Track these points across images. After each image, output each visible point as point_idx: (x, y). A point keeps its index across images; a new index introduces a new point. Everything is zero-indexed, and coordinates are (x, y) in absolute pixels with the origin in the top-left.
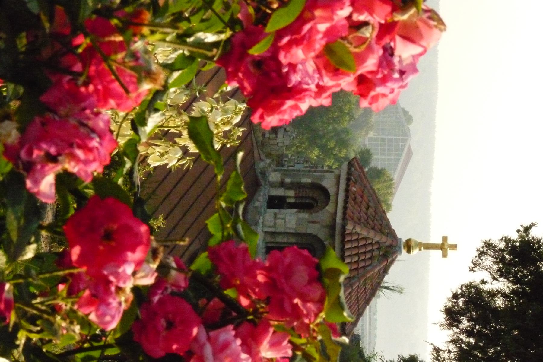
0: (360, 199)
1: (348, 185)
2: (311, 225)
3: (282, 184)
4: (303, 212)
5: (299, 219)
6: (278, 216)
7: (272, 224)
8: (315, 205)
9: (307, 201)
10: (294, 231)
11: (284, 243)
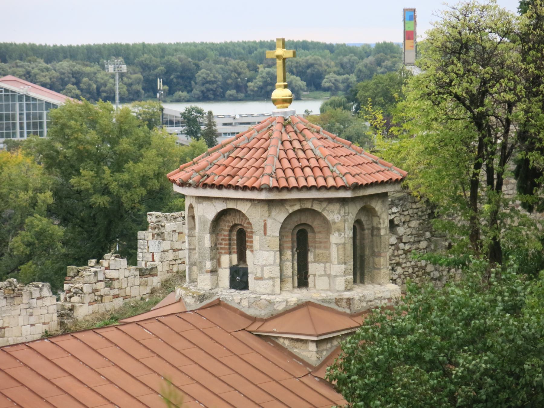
0: (229, 168)
1: (212, 186)
2: (268, 233)
3: (214, 271)
4: (252, 242)
5: (262, 248)
6: (259, 275)
7: (270, 282)
8: (240, 227)
9: (235, 238)
10: (278, 253)
11: (293, 264)
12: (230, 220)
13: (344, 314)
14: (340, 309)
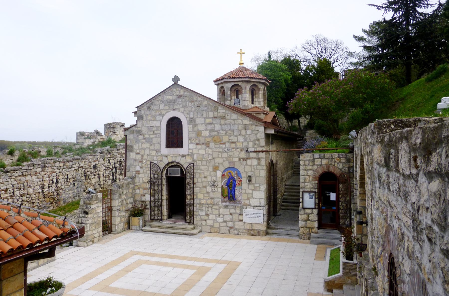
3: (230, 100)
12: (235, 88)
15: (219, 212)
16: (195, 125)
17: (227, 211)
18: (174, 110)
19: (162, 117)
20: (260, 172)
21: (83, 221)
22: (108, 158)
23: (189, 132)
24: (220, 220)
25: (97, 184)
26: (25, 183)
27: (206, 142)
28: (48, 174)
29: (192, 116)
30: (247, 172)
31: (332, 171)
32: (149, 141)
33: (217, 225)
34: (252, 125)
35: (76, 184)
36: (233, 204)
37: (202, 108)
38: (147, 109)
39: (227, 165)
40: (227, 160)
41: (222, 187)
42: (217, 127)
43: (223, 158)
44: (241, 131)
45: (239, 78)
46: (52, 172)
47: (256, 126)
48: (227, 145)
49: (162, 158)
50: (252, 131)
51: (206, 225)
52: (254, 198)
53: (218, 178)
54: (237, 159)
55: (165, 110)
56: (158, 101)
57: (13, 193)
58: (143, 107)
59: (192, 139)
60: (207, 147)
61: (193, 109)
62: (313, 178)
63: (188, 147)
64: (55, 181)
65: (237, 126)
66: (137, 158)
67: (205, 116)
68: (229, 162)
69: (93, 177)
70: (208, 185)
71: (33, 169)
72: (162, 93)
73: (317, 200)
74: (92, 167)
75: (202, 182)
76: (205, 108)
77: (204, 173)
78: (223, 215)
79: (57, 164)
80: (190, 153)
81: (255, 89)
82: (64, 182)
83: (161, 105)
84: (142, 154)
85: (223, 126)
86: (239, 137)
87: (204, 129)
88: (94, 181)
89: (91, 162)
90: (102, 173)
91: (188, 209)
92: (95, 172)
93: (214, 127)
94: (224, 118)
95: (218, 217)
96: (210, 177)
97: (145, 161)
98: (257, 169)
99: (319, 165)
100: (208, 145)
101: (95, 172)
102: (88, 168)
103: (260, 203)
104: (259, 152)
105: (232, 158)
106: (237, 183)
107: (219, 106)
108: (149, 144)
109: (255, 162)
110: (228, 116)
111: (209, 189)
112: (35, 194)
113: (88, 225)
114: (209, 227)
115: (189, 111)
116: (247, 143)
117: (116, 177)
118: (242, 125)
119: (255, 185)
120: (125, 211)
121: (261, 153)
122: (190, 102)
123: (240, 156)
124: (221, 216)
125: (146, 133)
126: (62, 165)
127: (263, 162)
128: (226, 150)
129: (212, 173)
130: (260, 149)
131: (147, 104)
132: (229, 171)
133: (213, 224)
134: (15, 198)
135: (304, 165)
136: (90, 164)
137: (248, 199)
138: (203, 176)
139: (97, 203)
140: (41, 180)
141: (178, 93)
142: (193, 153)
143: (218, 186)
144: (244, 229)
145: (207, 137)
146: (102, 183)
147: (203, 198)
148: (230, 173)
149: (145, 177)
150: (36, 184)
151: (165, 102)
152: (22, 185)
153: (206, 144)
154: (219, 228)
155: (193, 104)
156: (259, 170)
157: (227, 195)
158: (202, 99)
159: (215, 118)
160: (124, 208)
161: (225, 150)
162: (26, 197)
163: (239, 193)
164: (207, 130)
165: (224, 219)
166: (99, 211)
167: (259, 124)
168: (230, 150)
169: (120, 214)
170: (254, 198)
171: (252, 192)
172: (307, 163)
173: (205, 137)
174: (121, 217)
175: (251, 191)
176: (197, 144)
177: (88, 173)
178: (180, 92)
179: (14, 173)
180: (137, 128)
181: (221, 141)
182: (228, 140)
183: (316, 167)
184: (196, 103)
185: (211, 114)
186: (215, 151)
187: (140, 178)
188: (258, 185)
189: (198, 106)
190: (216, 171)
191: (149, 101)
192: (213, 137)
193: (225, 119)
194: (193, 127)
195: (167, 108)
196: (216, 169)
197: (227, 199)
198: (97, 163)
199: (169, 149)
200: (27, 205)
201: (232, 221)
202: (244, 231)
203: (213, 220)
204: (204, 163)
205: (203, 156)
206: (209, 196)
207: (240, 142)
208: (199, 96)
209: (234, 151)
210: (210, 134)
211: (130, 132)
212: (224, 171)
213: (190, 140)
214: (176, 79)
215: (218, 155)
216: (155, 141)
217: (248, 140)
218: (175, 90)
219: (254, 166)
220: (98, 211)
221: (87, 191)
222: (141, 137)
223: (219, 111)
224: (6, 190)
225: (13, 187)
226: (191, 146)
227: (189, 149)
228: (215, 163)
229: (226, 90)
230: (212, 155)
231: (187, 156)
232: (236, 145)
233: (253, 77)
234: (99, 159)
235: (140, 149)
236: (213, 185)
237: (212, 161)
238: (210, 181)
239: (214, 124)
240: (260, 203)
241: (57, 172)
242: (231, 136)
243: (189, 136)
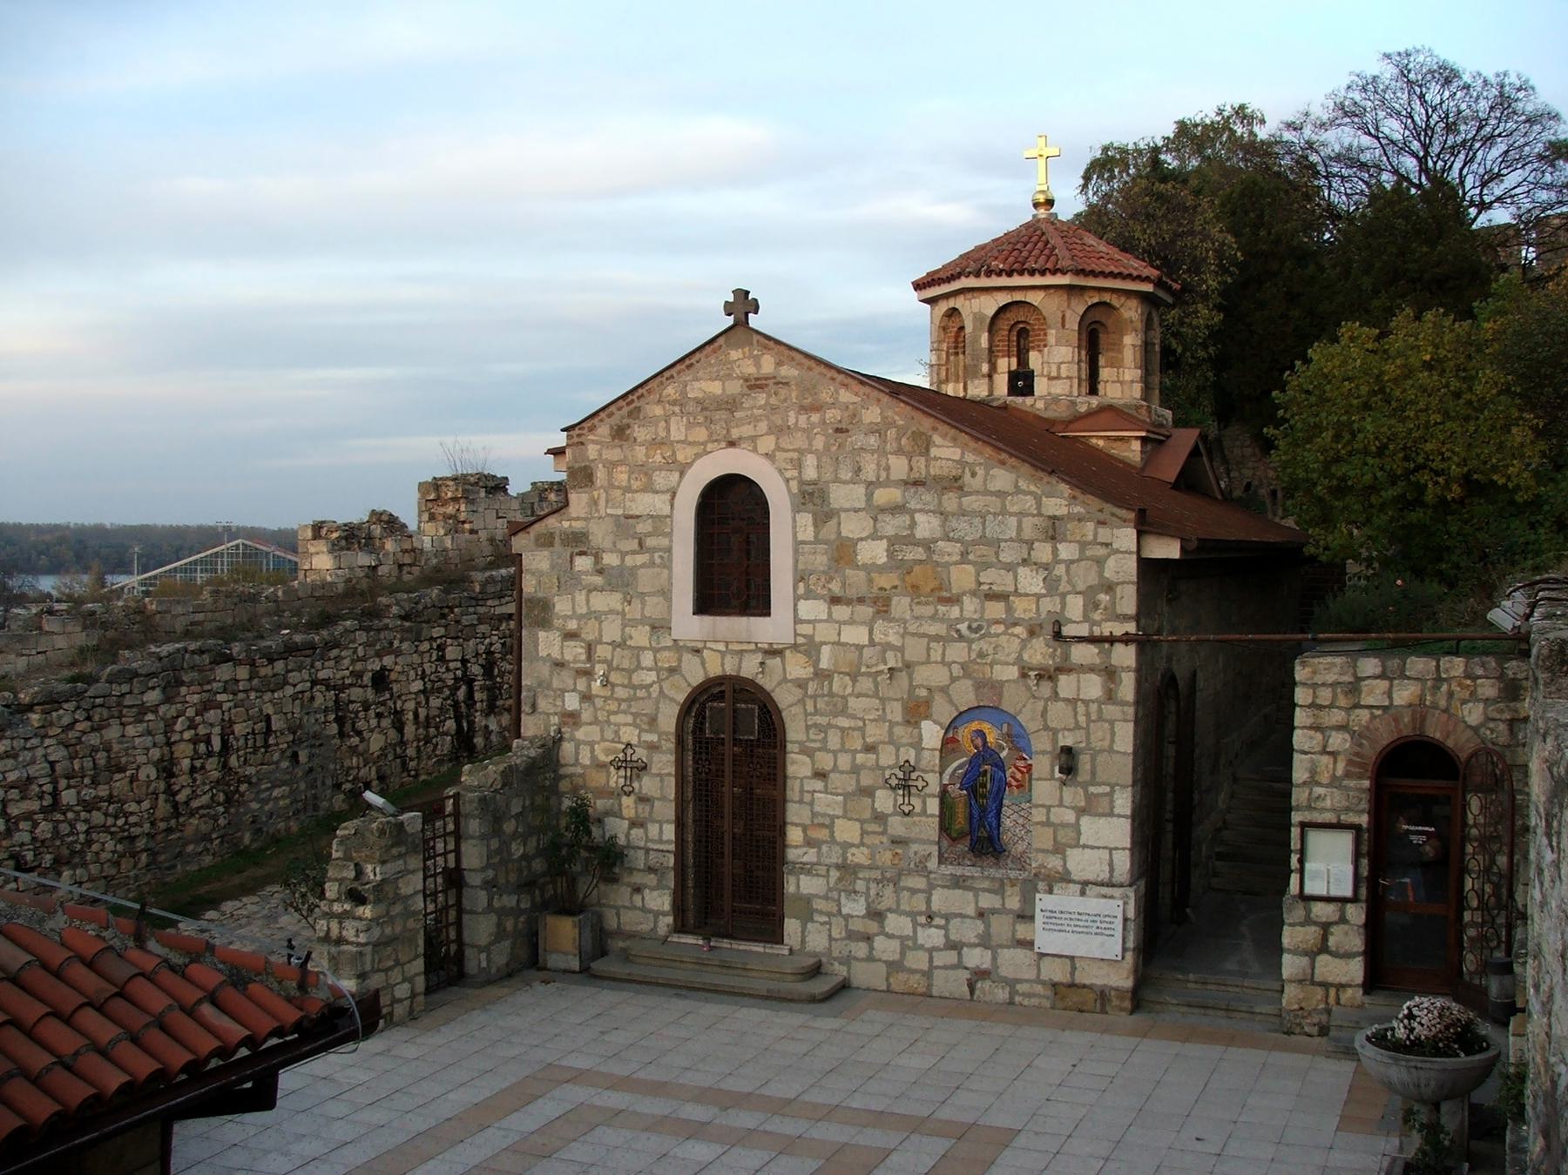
3: (990, 376)
6: (1054, 374)
7: (1068, 381)
12: (1011, 316)
13: (1144, 421)
14: (1141, 417)
15: (928, 901)
16: (825, 515)
17: (961, 901)
18: (732, 444)
19: (676, 475)
20: (1113, 734)
21: (344, 933)
22: (435, 639)
23: (797, 544)
24: (932, 937)
25: (390, 757)
26: (99, 755)
27: (875, 590)
28: (190, 712)
29: (810, 473)
30: (1055, 732)
31: (1438, 736)
32: (620, 580)
33: (918, 960)
34: (1080, 520)
35: (303, 756)
36: (993, 872)
37: (857, 439)
38: (613, 438)
39: (965, 695)
40: (967, 673)
41: (944, 794)
42: (926, 526)
43: (949, 665)
44: (1030, 544)
45: (1032, 273)
46: (205, 707)
47: (1102, 523)
48: (970, 605)
49: (680, 660)
50: (1083, 545)
51: (870, 958)
52: (1084, 847)
53: (926, 754)
54: (1013, 672)
55: (690, 444)
56: (659, 401)
57: (55, 794)
58: (591, 429)
59: (813, 579)
60: (878, 612)
61: (819, 443)
62: (1350, 762)
63: (795, 610)
64: (216, 744)
65: (1013, 521)
66: (568, 657)
67: (869, 472)
68: (979, 685)
69: (374, 722)
70: (881, 782)
71: (130, 692)
72: (678, 367)
73: (1365, 862)
74: (367, 678)
75: (855, 770)
76: (873, 440)
77: (862, 730)
78: (948, 917)
79: (224, 672)
80: (801, 640)
81: (1103, 325)
82: (256, 750)
83: (673, 419)
84: (590, 637)
85: (954, 523)
86: (1023, 572)
87: (864, 535)
88: (376, 743)
89: (364, 659)
90: (411, 705)
91: (790, 887)
92: (383, 703)
93: (913, 524)
94: (954, 484)
95: (923, 926)
96: (891, 748)
97: (600, 670)
98: (1100, 719)
99: (1377, 707)
100: (882, 605)
101: (383, 703)
102: (351, 685)
103: (1112, 870)
104: (1112, 640)
105: (991, 666)
106: (1009, 779)
107: (935, 429)
108: (619, 596)
109: (1093, 687)
110: (974, 475)
111: (884, 801)
112: (139, 802)
113: (369, 948)
114: (883, 969)
115: (800, 451)
116: (1058, 600)
117: (471, 723)
118: (1036, 520)
119: (1092, 789)
120: (519, 887)
121: (1119, 648)
122: (804, 409)
123: (1026, 657)
124: (938, 921)
125: (607, 544)
126: (243, 672)
127: (1127, 687)
128: (963, 627)
129: (899, 731)
130: (1118, 629)
131: (610, 416)
132: (975, 726)
133: (903, 954)
134: (61, 818)
135: (1309, 706)
136: (359, 666)
137: (1059, 849)
138: (858, 745)
139: (400, 856)
140: (160, 738)
141: (749, 369)
142: (817, 639)
143: (927, 790)
144: (1038, 981)
145: (881, 569)
146: (411, 752)
147: (857, 841)
148: (981, 734)
149: (603, 739)
150: (142, 759)
151: (691, 408)
152: (88, 763)
153: (875, 601)
154: (928, 974)
155: (815, 418)
156: (1112, 723)
157: (967, 828)
158: (856, 399)
159: (916, 483)
160: (513, 878)
161: (958, 631)
162: (106, 815)
163: (1021, 821)
164: (881, 538)
165: (952, 937)
166: (410, 891)
167: (1113, 515)
168: (979, 628)
169: (496, 904)
170: (1084, 847)
171: (1078, 820)
172: (1325, 696)
173: (870, 568)
174: (502, 913)
175: (1070, 816)
176: (835, 600)
177: (351, 707)
178: (758, 365)
179: (54, 714)
180: (566, 524)
181: (940, 589)
182: (973, 586)
183: (1364, 715)
184: (832, 415)
185: (899, 467)
186: (914, 634)
187: (578, 744)
188: (1107, 789)
189: (838, 430)
190: (917, 725)
191: (621, 403)
192: (905, 568)
193: (961, 488)
194: (816, 525)
195: (701, 434)
196: (916, 711)
197: (963, 846)
198: (388, 661)
199: (708, 620)
200: (110, 845)
201: (985, 942)
202: (1039, 989)
203: (902, 939)
204: (865, 684)
205: (861, 655)
206: (884, 833)
207: (1027, 595)
208: (845, 385)
209: (998, 635)
210: (891, 554)
211: (537, 539)
212: (952, 726)
213: (802, 579)
214: (743, 305)
215: (928, 649)
216: (646, 580)
217: (1064, 587)
218: (735, 354)
219: (1086, 703)
220: (405, 890)
221: (347, 786)
222: (583, 563)
223: (934, 452)
224: (24, 785)
225: (53, 770)
226: (812, 609)
227: (797, 621)
228: (912, 688)
229: (969, 329)
230: (901, 649)
231: (788, 653)
232: (1009, 609)
233: (1098, 269)
234: (396, 643)
235: (580, 618)
236: (905, 786)
237: (902, 679)
238: (890, 767)
239: (912, 513)
240: (1112, 870)
241: (226, 706)
242: (986, 566)
243: (796, 561)
